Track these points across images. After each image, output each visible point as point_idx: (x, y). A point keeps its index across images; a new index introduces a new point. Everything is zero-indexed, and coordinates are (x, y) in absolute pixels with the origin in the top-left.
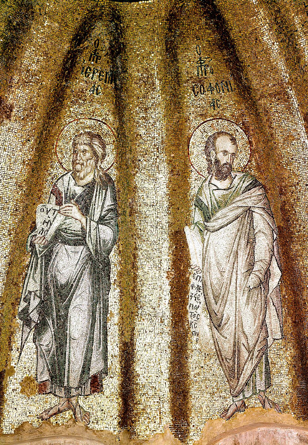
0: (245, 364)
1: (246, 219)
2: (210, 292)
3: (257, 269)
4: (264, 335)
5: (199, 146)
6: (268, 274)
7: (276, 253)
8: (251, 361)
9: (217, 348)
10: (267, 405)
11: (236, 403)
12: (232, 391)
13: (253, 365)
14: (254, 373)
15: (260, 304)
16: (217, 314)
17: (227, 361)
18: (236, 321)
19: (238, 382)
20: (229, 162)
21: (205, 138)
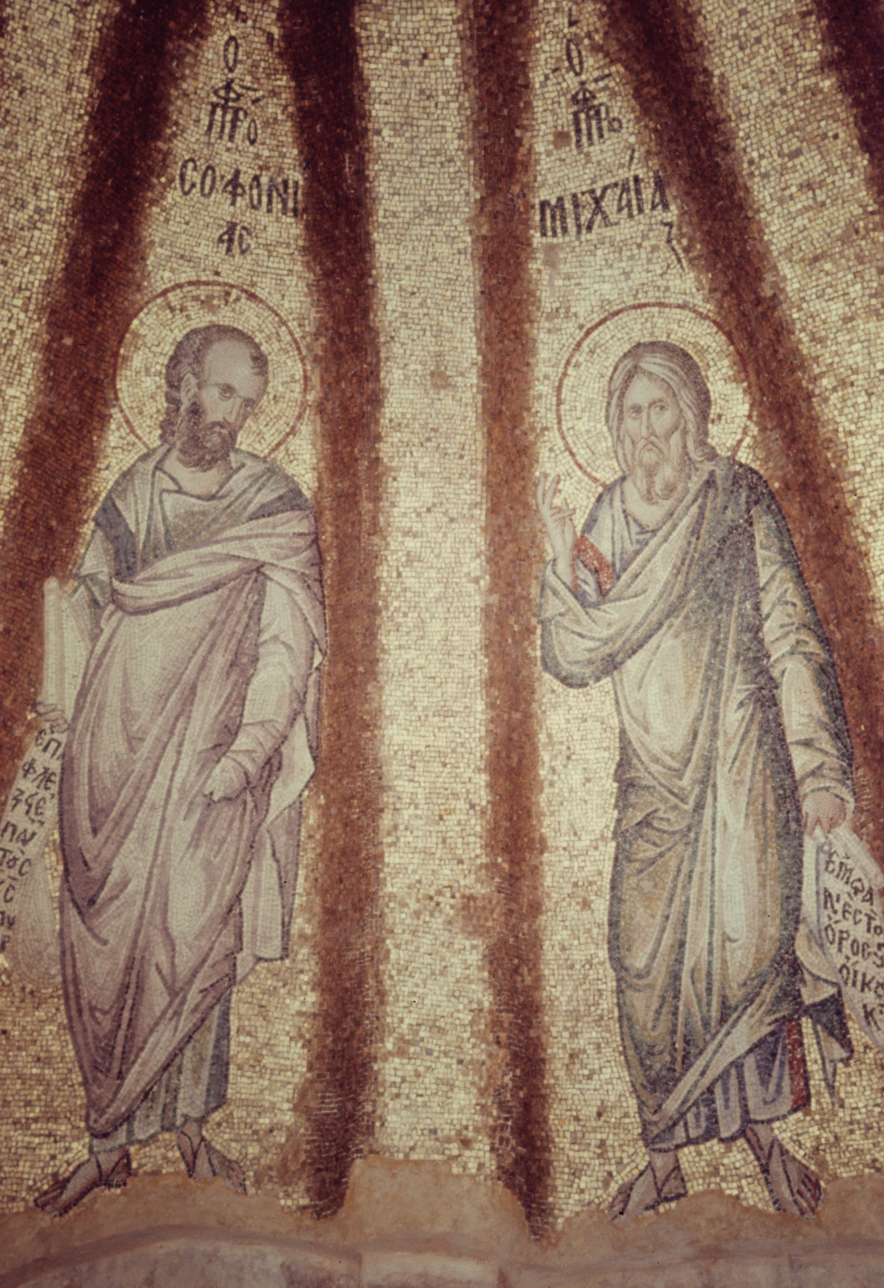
0: (151, 1031)
1: (244, 595)
2: (83, 791)
3: (244, 748)
4: (231, 941)
5: (154, 349)
6: (273, 764)
7: (309, 707)
8: (173, 1023)
9: (69, 971)
10: (202, 1165)
11: (102, 1158)
12: (93, 1116)
13: (179, 1035)
14: (177, 1060)
15: (233, 849)
16: (91, 865)
17: (93, 1016)
18: (147, 893)
19: (120, 1086)
20: (231, 419)
21: (176, 331)
